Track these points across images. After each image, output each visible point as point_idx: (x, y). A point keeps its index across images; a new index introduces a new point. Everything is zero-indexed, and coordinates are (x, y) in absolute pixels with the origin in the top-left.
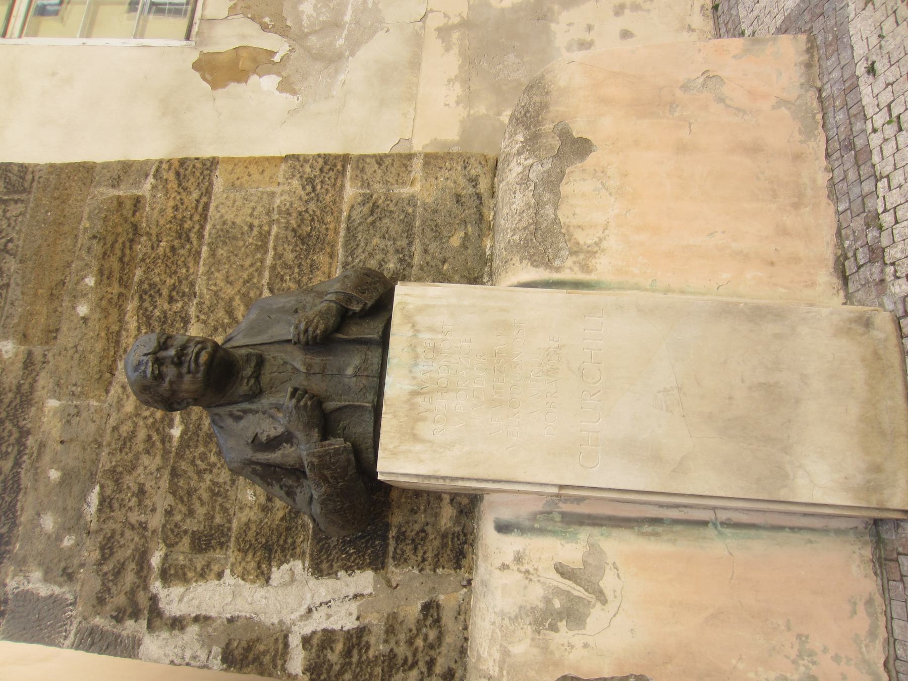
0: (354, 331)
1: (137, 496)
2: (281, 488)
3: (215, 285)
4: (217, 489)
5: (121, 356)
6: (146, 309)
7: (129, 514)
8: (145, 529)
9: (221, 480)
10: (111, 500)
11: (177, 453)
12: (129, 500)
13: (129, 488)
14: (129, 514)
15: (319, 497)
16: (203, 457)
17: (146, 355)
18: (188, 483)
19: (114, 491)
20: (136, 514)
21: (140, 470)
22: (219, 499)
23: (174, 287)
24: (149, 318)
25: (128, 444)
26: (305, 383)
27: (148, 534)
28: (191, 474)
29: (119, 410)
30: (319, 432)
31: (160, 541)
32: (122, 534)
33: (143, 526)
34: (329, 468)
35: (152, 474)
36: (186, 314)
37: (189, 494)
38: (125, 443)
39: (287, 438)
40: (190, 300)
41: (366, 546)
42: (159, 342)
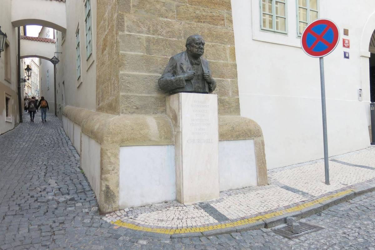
0: (207, 85)
32: (147, 26)
34: (179, 81)
35: (162, 33)
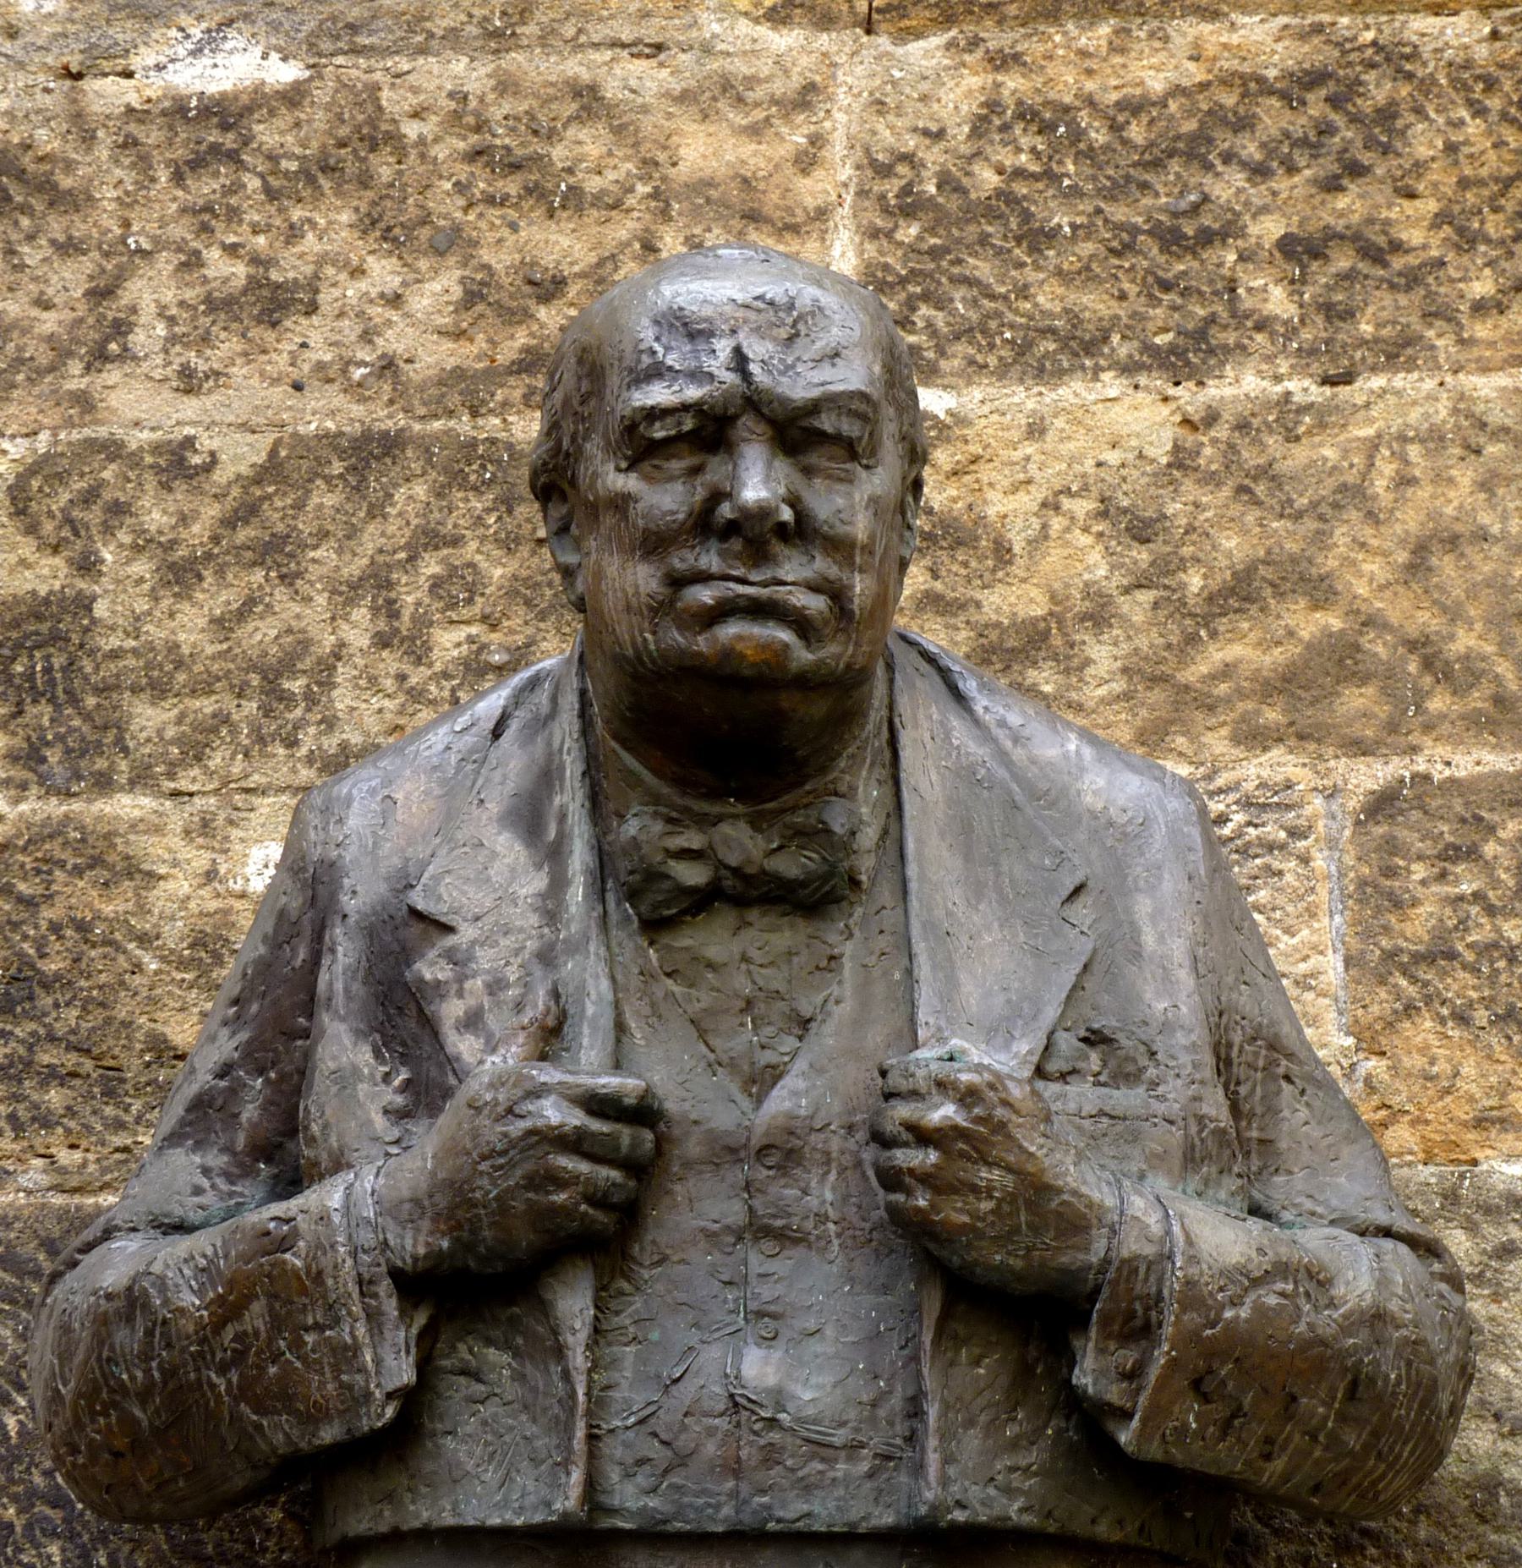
1: (253, 284)
2: (224, 1071)
3: (1404, 481)
4: (296, 686)
5: (975, 42)
6: (1244, 124)
7: (166, 262)
8: (99, 358)
9: (342, 699)
10: (233, 157)
11: (473, 444)
12: (232, 250)
13: (293, 234)
14: (166, 262)
15: (161, 1283)
16: (458, 588)
17: (740, 360)
18: (323, 535)
19: (272, 158)
20: (169, 296)
21: (383, 272)
22: (251, 707)
23: (1376, 250)
24: (1195, 150)
25: (511, 186)
26: (693, 1147)
27: (75, 379)
28: (371, 539)
29: (684, 97)
30: (436, 1256)
31: (43, 441)
32: (68, 248)
33: (107, 343)
34: (277, 1324)
35: (367, 337)
36: (1227, 352)
37: (279, 555)
38: (516, 167)
39: (428, 1089)
40: (1309, 353)
41: (32, 1494)
42: (814, 407)
